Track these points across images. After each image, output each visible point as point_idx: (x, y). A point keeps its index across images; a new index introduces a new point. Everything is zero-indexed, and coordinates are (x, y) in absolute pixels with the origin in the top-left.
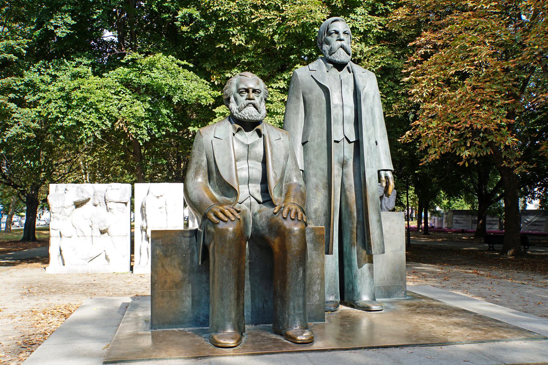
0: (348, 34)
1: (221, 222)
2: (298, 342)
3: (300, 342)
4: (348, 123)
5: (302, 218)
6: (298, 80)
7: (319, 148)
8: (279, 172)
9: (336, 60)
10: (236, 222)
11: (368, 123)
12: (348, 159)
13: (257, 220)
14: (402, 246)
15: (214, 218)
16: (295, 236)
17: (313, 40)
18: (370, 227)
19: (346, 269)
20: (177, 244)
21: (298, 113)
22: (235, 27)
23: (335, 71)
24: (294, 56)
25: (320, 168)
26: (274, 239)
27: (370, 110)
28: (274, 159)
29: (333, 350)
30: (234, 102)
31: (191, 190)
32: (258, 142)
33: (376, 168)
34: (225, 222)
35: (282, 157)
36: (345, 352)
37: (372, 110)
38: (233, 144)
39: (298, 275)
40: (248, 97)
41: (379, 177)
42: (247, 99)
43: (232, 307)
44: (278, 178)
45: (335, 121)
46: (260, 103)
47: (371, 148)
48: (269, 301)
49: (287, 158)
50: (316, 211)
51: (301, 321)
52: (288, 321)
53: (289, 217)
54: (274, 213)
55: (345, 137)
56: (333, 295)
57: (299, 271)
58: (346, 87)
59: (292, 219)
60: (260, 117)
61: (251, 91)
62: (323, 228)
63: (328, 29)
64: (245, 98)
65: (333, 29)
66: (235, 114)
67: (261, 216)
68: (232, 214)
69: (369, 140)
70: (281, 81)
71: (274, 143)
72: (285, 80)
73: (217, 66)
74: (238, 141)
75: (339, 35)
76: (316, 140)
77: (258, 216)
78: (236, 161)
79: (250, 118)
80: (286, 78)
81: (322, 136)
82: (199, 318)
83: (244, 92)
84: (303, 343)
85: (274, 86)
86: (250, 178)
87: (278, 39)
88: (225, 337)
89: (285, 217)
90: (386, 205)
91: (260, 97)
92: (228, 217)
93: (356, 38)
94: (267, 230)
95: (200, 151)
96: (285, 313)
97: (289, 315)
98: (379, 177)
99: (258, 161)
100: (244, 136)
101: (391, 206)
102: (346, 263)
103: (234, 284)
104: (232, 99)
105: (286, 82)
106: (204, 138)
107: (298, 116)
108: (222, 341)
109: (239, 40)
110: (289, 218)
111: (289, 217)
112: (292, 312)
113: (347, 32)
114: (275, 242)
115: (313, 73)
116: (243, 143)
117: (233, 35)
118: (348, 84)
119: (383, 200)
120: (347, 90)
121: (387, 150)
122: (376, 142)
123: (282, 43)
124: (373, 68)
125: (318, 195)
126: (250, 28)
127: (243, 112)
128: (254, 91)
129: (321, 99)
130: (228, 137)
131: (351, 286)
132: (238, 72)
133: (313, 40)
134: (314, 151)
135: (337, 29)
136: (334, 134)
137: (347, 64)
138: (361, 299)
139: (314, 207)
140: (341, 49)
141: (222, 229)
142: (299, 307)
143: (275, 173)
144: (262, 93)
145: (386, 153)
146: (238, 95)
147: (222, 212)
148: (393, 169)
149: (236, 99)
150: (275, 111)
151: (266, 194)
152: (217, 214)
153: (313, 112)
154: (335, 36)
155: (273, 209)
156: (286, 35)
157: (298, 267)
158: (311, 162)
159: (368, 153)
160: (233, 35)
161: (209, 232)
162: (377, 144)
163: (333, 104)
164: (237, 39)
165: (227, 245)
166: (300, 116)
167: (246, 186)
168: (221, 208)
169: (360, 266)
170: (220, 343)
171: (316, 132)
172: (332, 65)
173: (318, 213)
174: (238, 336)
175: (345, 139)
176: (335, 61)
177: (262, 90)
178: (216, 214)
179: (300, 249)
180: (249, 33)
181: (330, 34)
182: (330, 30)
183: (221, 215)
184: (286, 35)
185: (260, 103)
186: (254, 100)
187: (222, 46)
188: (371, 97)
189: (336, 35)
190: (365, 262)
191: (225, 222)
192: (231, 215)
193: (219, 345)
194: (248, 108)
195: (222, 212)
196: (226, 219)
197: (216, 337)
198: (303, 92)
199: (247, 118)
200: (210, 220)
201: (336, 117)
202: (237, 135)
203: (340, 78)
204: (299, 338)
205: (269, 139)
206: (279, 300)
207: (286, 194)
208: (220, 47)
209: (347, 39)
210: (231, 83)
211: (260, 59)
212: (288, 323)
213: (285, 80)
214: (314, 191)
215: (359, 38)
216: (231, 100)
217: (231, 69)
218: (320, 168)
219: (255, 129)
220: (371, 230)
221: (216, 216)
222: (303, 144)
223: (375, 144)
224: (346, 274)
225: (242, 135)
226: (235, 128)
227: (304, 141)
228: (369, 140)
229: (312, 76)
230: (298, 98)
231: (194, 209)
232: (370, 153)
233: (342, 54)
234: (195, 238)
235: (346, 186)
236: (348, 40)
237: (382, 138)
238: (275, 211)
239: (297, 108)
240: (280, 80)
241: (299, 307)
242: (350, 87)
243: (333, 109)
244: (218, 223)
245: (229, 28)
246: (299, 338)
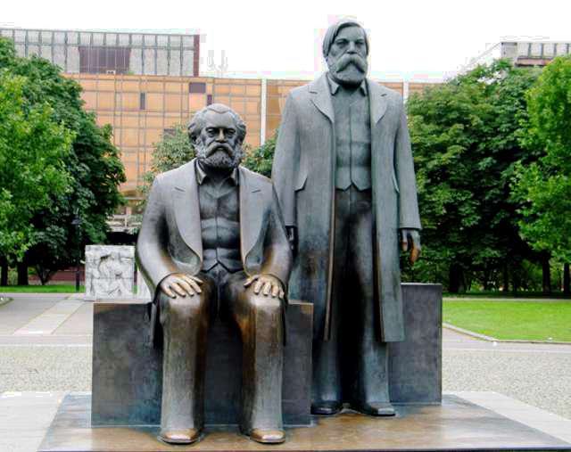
1: (178, 297)
34: (184, 296)
41: (400, 237)
55: (353, 184)
59: (266, 295)
68: (191, 286)
89: (257, 291)
114: (244, 322)
116: (211, 196)
137: (360, 83)
192: (189, 288)
246: (264, 437)
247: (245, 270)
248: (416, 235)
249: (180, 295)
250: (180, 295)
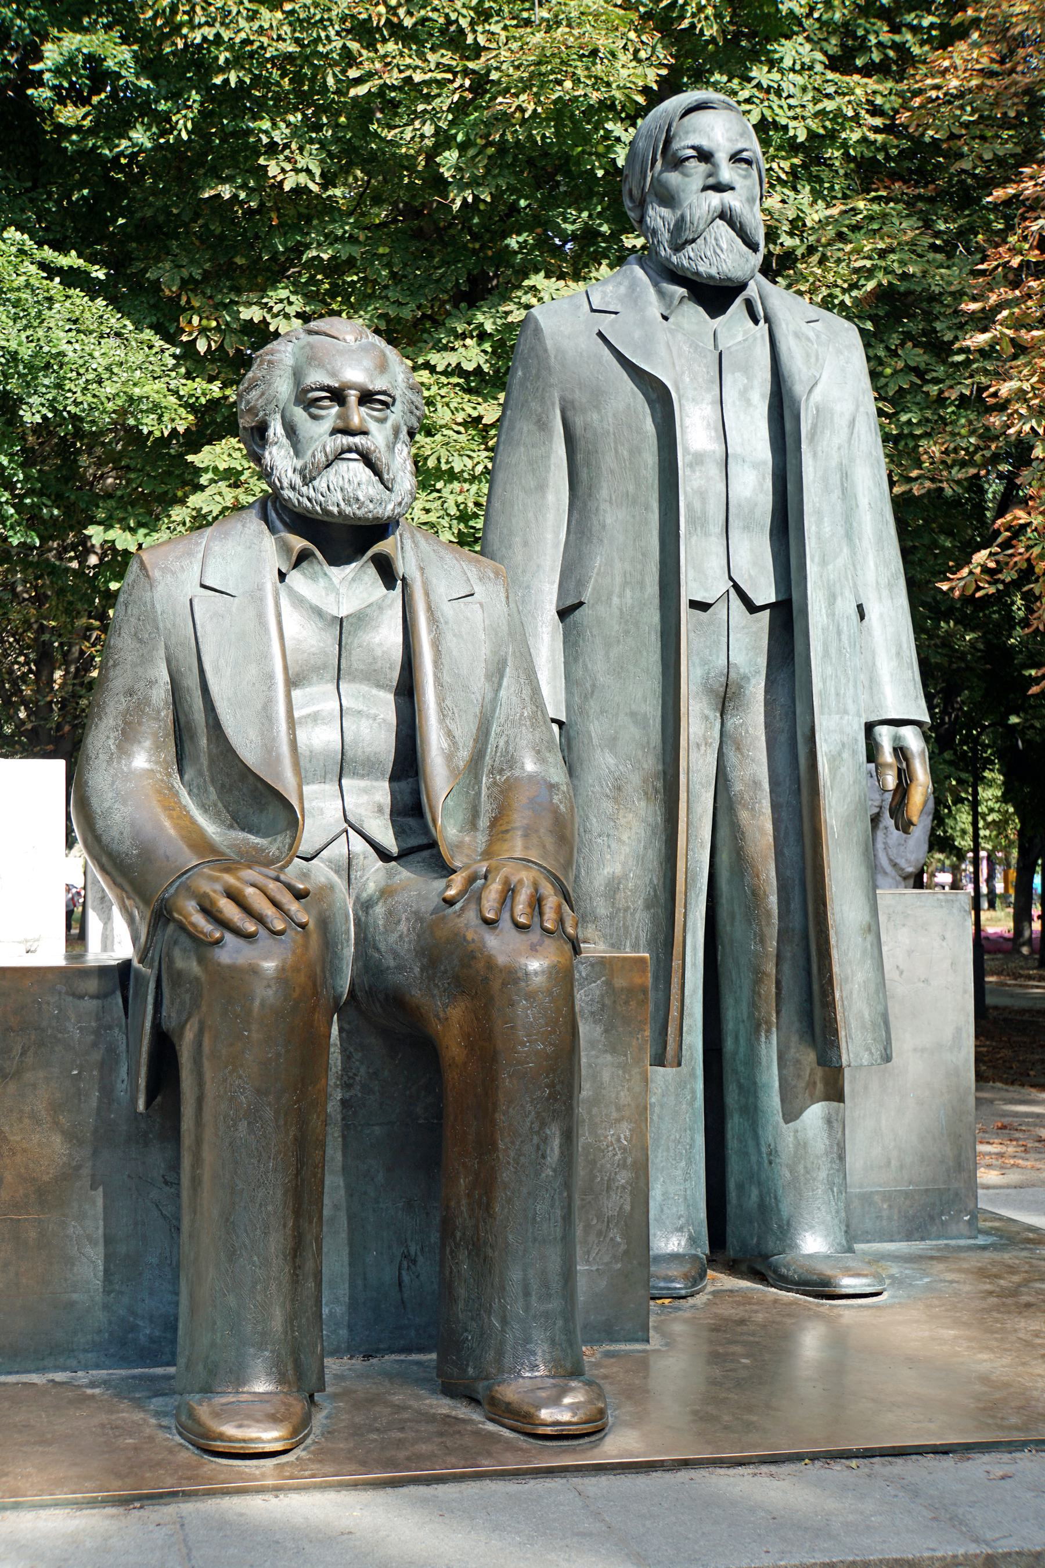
0: (748, 162)
2: (541, 1430)
3: (548, 1430)
4: (747, 528)
5: (561, 921)
6: (546, 350)
7: (627, 632)
8: (465, 731)
9: (701, 269)
10: (294, 935)
11: (827, 529)
12: (746, 678)
13: (376, 926)
14: (959, 1030)
16: (530, 996)
17: (600, 173)
18: (834, 953)
19: (734, 1124)
20: (44, 1024)
21: (541, 487)
22: (279, 114)
23: (694, 314)
24: (521, 239)
25: (633, 714)
26: (446, 1006)
27: (835, 479)
28: (447, 678)
29: (685, 1464)
30: (285, 441)
31: (106, 805)
32: (380, 606)
33: (859, 716)
34: (249, 937)
35: (480, 671)
36: (732, 1471)
37: (845, 475)
38: (279, 615)
39: (544, 1157)
40: (340, 424)
42: (335, 431)
43: (273, 1287)
44: (464, 754)
45: (692, 520)
46: (391, 448)
47: (839, 633)
48: (421, 1259)
49: (497, 673)
50: (613, 887)
51: (553, 1342)
52: (503, 1343)
53: (506, 916)
54: (445, 900)
55: (736, 587)
56: (680, 1229)
57: (545, 1140)
58: (741, 380)
60: (390, 507)
61: (353, 396)
62: (642, 960)
63: (668, 142)
64: (327, 425)
65: (690, 143)
66: (287, 493)
67: (390, 913)
68: (276, 904)
69: (832, 599)
70: (468, 342)
71: (447, 610)
72: (482, 336)
73: (206, 275)
74: (299, 601)
75: (715, 165)
76: (615, 600)
77: (379, 910)
78: (291, 683)
79: (348, 510)
80: (489, 327)
81: (642, 584)
82: (134, 1328)
83: (327, 403)
84: (563, 1436)
85: (440, 360)
86: (349, 754)
87: (458, 169)
88: (243, 1415)
89: (490, 915)
90: (893, 853)
91: (389, 424)
93: (775, 165)
94: (417, 970)
95: (140, 641)
96: (489, 1313)
97: (504, 1321)
98: (872, 752)
99: (379, 686)
100: (322, 582)
101: (912, 857)
102: (732, 1097)
103: (279, 1193)
104: (276, 429)
105: (487, 346)
106: (160, 591)
107: (543, 497)
108: (230, 1430)
109: (297, 171)
110: (506, 923)
111: (506, 916)
112: (517, 1308)
113: (745, 155)
115: (605, 323)
116: (318, 612)
117: (272, 149)
118: (746, 369)
119: (880, 834)
120: (744, 393)
121: (904, 639)
122: (860, 608)
123: (475, 183)
124: (844, 291)
125: (623, 821)
126: (342, 119)
127: (321, 483)
128: (367, 398)
129: (639, 431)
130: (260, 588)
131: (755, 1193)
132: (290, 303)
133: (600, 173)
134: (608, 646)
135: (705, 143)
136: (691, 574)
137: (743, 286)
138: (794, 1246)
139: (607, 871)
140: (721, 226)
141: (233, 968)
142: (546, 1285)
143: (449, 734)
144: (398, 408)
145: (898, 654)
146: (299, 414)
147: (234, 896)
148: (927, 719)
149: (291, 431)
150: (444, 467)
151: (411, 822)
152: (213, 903)
153: (605, 485)
154: (698, 169)
155: (441, 883)
156: (491, 150)
157: (543, 1124)
158: (594, 686)
159: (826, 653)
160: (272, 149)
161: (178, 978)
162: (862, 617)
163: (686, 450)
164: (288, 167)
165: (256, 1034)
166: (551, 498)
167: (332, 788)
168: (230, 879)
169: (791, 1115)
170: (221, 1437)
171: (618, 565)
172: (681, 291)
173: (620, 895)
174: (298, 1407)
175: (733, 594)
176: (697, 273)
177: (397, 393)
178: (207, 905)
179: (550, 1049)
180: (336, 140)
181: (677, 163)
182: (675, 145)
183: (230, 910)
184: (491, 150)
185: (391, 448)
186: (365, 433)
187: (226, 191)
188: (841, 422)
189: (702, 167)
190: (811, 1096)
191: (249, 937)
192: (269, 911)
193: (219, 1445)
194: (341, 466)
195: (234, 896)
196: (251, 927)
197: (203, 1412)
198: (562, 399)
199: (335, 510)
200: (182, 927)
201: (697, 505)
202: (295, 578)
203: (716, 346)
204: (546, 1414)
205: (427, 594)
206: (463, 1255)
207: (494, 823)
208: (218, 196)
209: (748, 182)
210: (270, 362)
211: (381, 250)
212: (500, 1354)
213: (482, 336)
214: (608, 806)
215: (786, 165)
216: (271, 432)
217: (263, 290)
218: (633, 714)
219: (370, 553)
220: (836, 969)
221: (209, 911)
222: (563, 614)
223: (855, 617)
224: (732, 1143)
225: (314, 578)
226: (285, 548)
227: (569, 602)
228: (832, 599)
229: (600, 334)
230: (543, 425)
231: (119, 880)
232: (833, 651)
233: (724, 246)
234: (120, 1001)
235: (738, 787)
236: (750, 189)
237: (885, 593)
238: (451, 892)
239: (539, 465)
240: (463, 336)
241: (547, 1287)
242: (756, 383)
243: (688, 472)
244: (218, 942)
245: (255, 117)
247: (443, 850)
248: (913, 740)
249: (238, 932)
250: (238, 932)
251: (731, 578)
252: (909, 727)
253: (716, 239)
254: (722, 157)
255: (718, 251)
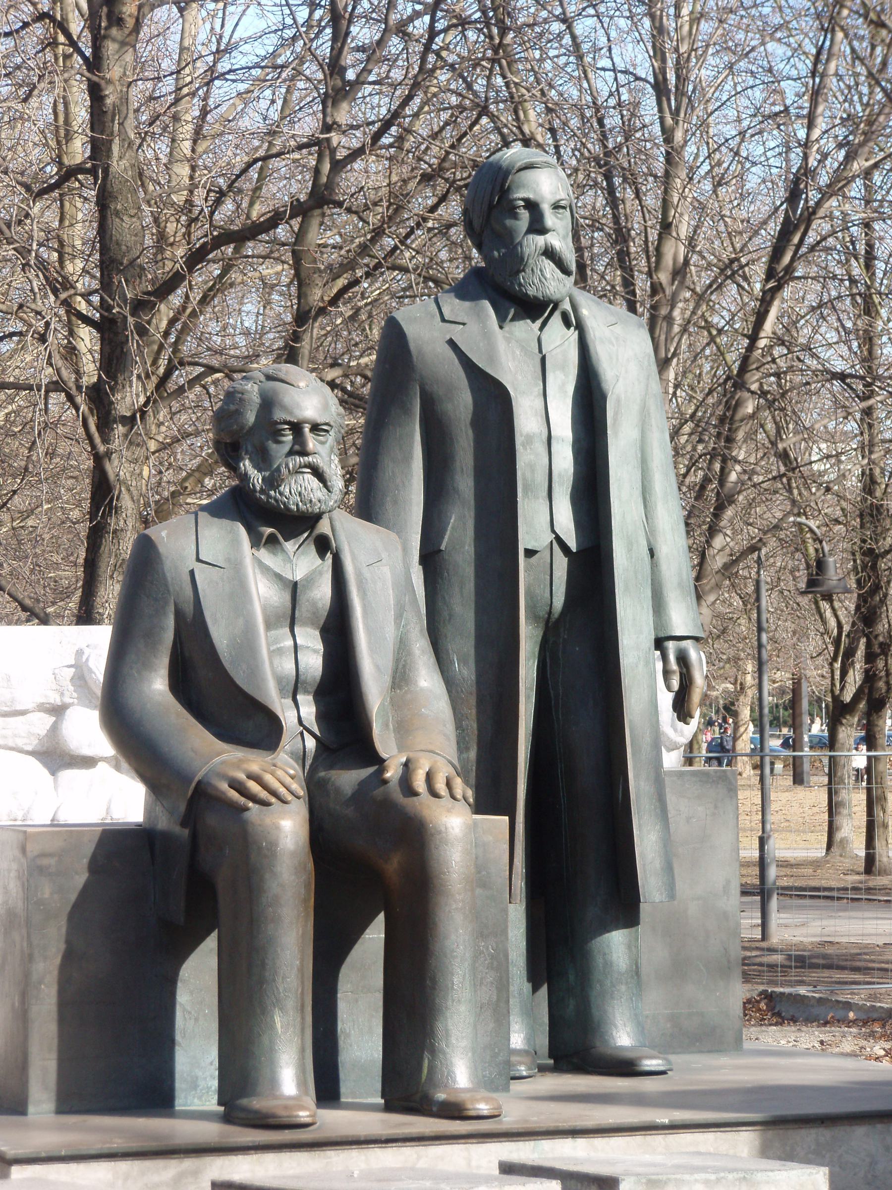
15: (234, 795)
45: (526, 488)
55: (558, 539)
58: (560, 375)
61: (307, 429)
71: (367, 573)
86: (302, 678)
91: (328, 445)
92: (274, 793)
116: (279, 577)
118: (563, 367)
188: (635, 408)
199: (294, 508)
201: (528, 475)
203: (540, 351)
251: (553, 531)
252: (689, 642)
253: (541, 271)
254: (546, 208)
255: (543, 280)
